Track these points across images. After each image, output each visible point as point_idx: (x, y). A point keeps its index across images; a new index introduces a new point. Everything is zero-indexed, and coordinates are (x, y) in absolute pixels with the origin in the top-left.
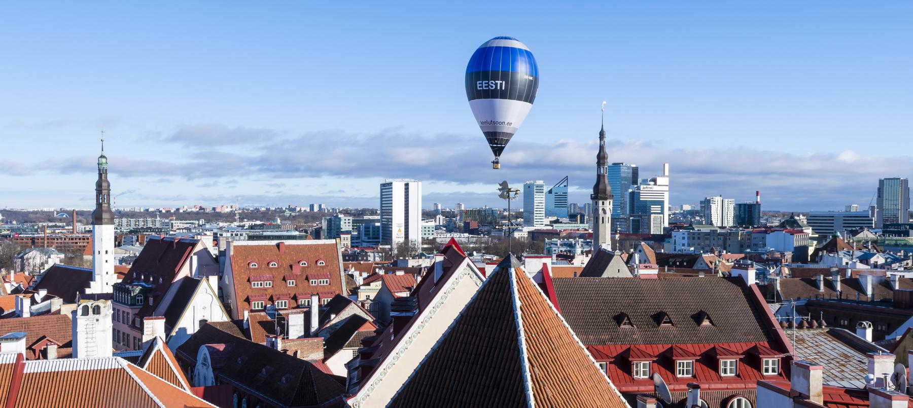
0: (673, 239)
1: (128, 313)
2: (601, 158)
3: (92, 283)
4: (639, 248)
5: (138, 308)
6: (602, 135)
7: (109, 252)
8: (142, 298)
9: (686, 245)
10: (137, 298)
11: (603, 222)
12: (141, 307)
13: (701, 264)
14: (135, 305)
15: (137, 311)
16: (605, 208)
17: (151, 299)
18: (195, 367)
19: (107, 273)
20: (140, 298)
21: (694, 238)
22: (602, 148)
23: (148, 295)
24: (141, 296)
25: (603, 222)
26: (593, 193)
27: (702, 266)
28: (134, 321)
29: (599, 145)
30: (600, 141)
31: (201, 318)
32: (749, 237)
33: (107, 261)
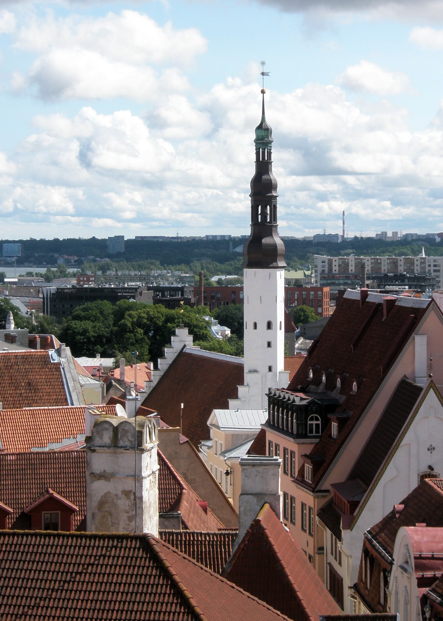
1: (292, 453)
3: (241, 390)
5: (312, 443)
7: (273, 327)
8: (319, 422)
10: (309, 422)
12: (317, 440)
14: (305, 436)
15: (308, 450)
17: (334, 425)
18: (390, 572)
19: (270, 369)
20: (314, 422)
23: (329, 416)
24: (317, 419)
28: (302, 470)
31: (424, 469)
33: (269, 345)
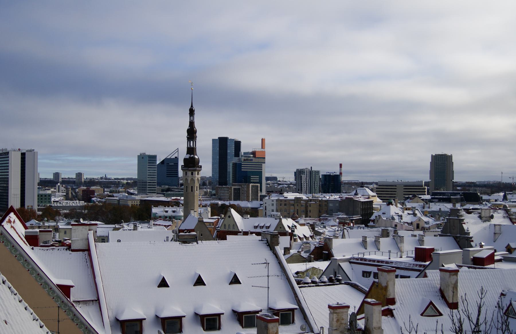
0: (265, 205)
2: (192, 134)
4: (228, 214)
6: (192, 112)
9: (275, 210)
11: (192, 191)
13: (281, 228)
16: (194, 178)
21: (281, 205)
22: (192, 124)
25: (192, 191)
26: (183, 165)
27: (281, 229)
29: (189, 121)
30: (190, 116)
32: (326, 203)
